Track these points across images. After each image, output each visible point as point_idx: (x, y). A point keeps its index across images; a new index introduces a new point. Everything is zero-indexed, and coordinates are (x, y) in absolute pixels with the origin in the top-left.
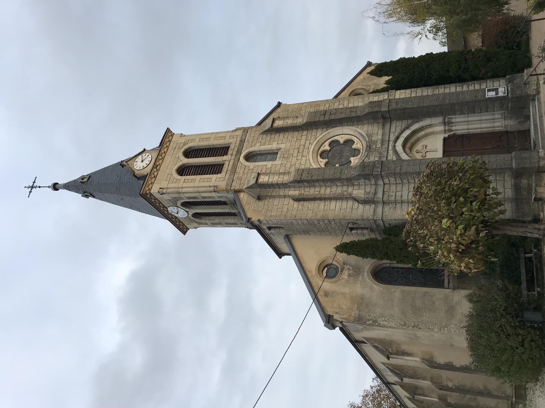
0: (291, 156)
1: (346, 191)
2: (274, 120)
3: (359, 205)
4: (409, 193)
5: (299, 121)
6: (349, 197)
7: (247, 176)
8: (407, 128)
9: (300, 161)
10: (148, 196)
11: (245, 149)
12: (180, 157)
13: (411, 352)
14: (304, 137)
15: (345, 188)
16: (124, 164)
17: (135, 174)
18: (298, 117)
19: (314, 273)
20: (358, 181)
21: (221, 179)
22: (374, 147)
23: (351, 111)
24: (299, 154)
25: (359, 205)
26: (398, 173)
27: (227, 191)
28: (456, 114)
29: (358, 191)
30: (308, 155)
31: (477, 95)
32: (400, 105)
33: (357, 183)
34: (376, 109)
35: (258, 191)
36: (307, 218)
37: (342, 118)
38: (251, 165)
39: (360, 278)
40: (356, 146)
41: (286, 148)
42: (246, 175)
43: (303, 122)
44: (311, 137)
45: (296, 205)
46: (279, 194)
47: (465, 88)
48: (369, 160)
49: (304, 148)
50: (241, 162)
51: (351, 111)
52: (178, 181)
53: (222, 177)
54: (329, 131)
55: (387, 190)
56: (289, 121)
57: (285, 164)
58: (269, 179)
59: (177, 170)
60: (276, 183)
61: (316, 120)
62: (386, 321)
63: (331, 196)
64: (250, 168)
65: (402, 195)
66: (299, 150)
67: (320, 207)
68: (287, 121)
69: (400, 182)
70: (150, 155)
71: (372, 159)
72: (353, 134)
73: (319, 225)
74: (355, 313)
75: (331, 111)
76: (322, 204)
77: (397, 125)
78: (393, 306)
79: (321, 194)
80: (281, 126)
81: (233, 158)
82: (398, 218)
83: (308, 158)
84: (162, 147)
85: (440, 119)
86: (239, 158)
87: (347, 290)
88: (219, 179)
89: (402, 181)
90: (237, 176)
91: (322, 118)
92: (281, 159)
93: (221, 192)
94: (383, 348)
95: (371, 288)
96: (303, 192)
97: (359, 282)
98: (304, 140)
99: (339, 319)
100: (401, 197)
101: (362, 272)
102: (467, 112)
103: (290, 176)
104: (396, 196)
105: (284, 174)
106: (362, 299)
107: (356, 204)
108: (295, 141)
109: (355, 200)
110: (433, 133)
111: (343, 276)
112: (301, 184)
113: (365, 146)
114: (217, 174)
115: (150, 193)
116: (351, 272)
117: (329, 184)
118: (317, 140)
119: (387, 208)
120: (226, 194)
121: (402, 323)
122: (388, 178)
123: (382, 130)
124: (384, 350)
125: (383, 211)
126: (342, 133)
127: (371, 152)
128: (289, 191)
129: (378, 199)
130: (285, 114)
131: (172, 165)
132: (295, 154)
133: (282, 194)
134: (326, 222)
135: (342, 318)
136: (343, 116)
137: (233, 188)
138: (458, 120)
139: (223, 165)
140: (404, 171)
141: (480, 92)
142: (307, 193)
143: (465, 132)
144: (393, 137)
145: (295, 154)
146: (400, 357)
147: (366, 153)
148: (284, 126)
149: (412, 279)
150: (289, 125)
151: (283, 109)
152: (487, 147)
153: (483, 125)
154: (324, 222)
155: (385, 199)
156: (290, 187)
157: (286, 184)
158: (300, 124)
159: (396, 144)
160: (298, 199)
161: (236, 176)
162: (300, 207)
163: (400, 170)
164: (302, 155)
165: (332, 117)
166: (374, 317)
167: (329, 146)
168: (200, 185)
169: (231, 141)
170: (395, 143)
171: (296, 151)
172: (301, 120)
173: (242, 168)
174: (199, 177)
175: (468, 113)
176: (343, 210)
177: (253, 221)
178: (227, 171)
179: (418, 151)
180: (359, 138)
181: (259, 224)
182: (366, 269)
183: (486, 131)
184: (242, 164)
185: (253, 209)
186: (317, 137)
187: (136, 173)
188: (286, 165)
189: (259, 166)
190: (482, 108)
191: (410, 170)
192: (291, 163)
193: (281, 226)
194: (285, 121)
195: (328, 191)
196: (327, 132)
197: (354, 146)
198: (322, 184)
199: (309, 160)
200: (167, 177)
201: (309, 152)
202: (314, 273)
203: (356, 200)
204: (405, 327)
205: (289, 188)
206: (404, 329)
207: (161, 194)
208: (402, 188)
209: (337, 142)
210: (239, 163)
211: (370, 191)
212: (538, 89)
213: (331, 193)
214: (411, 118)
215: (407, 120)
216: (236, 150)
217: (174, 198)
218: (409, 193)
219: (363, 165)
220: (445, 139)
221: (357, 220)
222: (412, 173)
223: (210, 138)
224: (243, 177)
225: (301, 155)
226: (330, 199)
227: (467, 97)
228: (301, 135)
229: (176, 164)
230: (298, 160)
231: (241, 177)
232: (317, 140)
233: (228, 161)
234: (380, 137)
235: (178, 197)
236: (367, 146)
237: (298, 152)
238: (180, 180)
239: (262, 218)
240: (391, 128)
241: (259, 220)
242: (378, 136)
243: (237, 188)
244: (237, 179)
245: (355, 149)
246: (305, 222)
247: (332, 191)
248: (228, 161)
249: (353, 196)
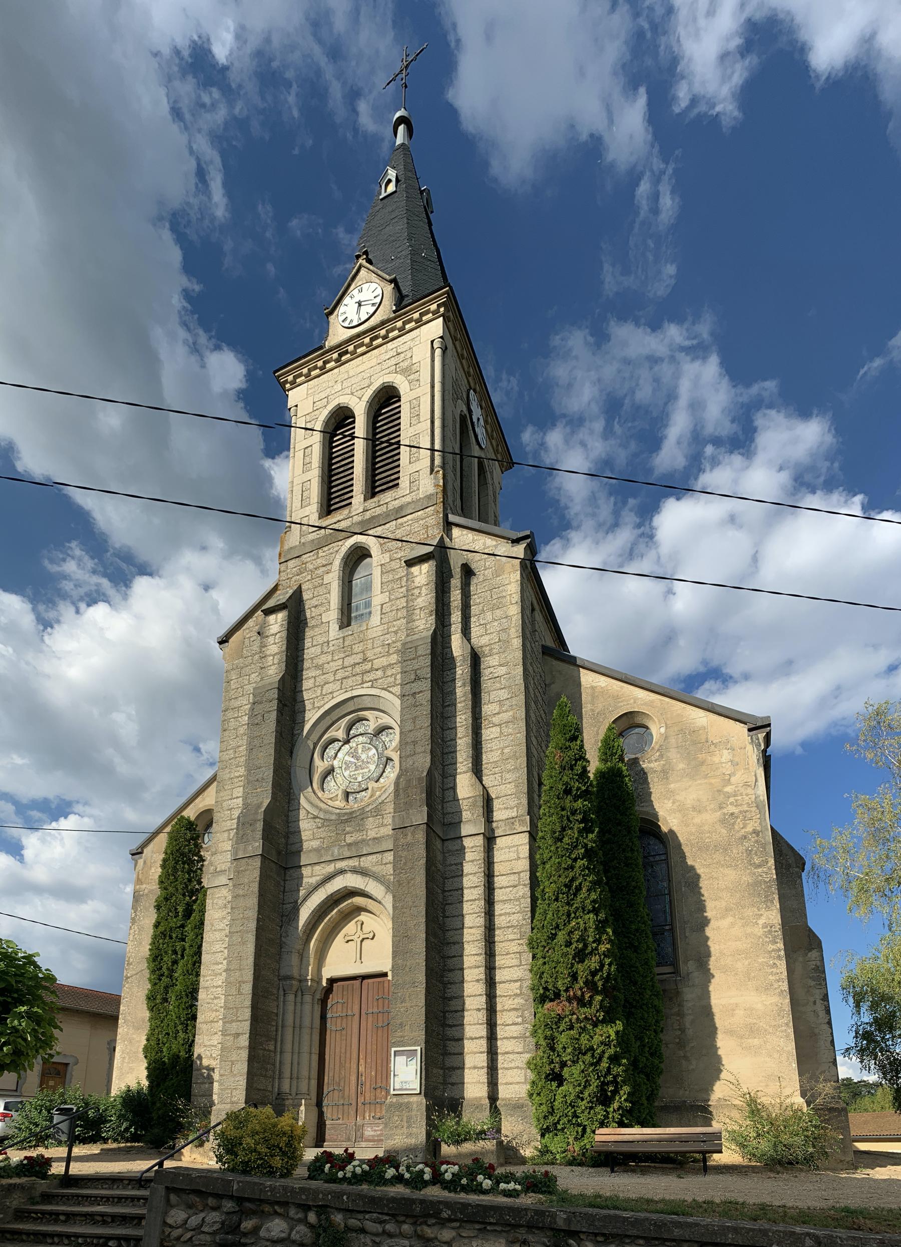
24: (351, 668)
66: (358, 664)
171: (358, 658)
184: (337, 551)
199: (333, 698)
201: (352, 690)
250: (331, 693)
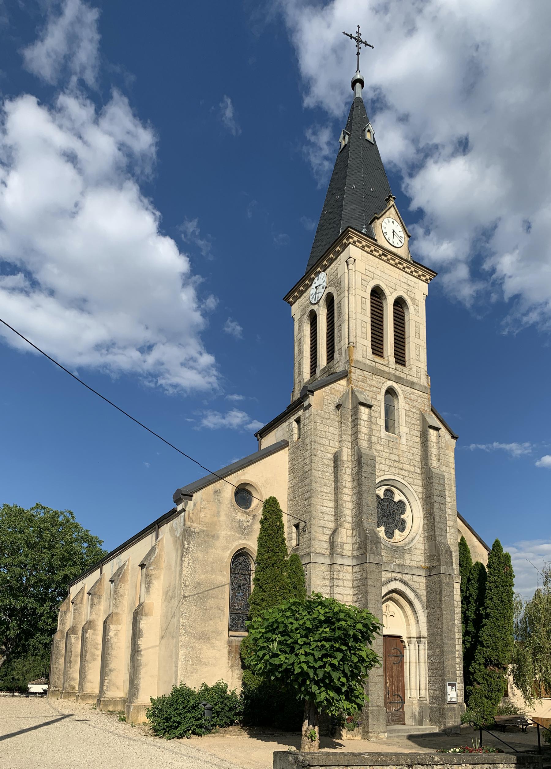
0: (391, 451)
1: (345, 521)
2: (437, 429)
3: (328, 536)
4: (342, 594)
5: (434, 463)
6: (337, 523)
7: (368, 390)
8: (417, 595)
9: (384, 462)
10: (345, 241)
11: (402, 389)
12: (396, 291)
13: (151, 591)
14: (412, 468)
15: (349, 519)
16: (391, 202)
17: (376, 221)
18: (439, 461)
19: (242, 478)
20: (357, 534)
21: (364, 353)
22: (396, 556)
23: (442, 529)
24: (393, 462)
25: (328, 536)
26: (367, 582)
27: (349, 361)
28: (429, 650)
29: (345, 535)
30: (390, 473)
32: (446, 587)
33: (354, 534)
34: (443, 560)
35: (349, 405)
36: (313, 471)
37: (434, 518)
38: (381, 397)
39: (237, 535)
40: (398, 535)
41: (401, 445)
42: (368, 388)
43: (433, 468)
44: (412, 478)
45: (329, 456)
46: (344, 434)
47: (458, 660)
49: (400, 469)
50: (385, 382)
51: (442, 529)
52: (364, 287)
53: (368, 355)
54: (418, 501)
55: (345, 569)
56: (435, 450)
57: (381, 443)
58: (364, 420)
59: (379, 287)
60: (358, 430)
61: (434, 484)
62: (188, 564)
63: (340, 502)
64: (377, 395)
65: (339, 586)
66: (397, 461)
67: (326, 487)
68: (435, 447)
69: (355, 585)
70: (402, 244)
71: (383, 553)
72: (413, 531)
73: (303, 485)
74: (196, 527)
75: (443, 504)
76: (331, 490)
77: (420, 584)
78: (207, 572)
79: (342, 489)
80: (429, 439)
81: (392, 371)
82: (312, 581)
83: (386, 473)
84: (412, 264)
85: (424, 632)
86: (390, 380)
87: (223, 518)
88: (365, 350)
89: (356, 587)
90: (368, 377)
91: (435, 492)
92: (387, 438)
93: (347, 353)
94: (153, 559)
95: (225, 548)
96: (345, 466)
97: (233, 533)
98: (409, 469)
99: (187, 507)
100: (337, 586)
101: (245, 538)
102: (430, 661)
103: (367, 449)
104: (338, 579)
105: (370, 441)
106: (213, 536)
107: (329, 532)
108: (409, 457)
109: (335, 532)
110: (408, 624)
111: (239, 514)
112: (355, 463)
113: (398, 545)
114: (372, 348)
115: (349, 244)
116: (245, 524)
117: (355, 499)
118: (409, 486)
119: (324, 568)
120: (343, 360)
121: (187, 583)
122: (360, 571)
124: (151, 561)
126: (414, 517)
128: (347, 448)
129: (335, 558)
130: (443, 445)
131: (386, 280)
132: (392, 457)
133: (343, 438)
134: (307, 495)
135: (189, 512)
136: (437, 519)
137: (353, 369)
138: (422, 652)
139: (382, 357)
140: (369, 590)
142: (344, 471)
143: (406, 659)
144: (406, 578)
145: (392, 457)
146: (144, 579)
147: (389, 546)
148: (429, 442)
149: (237, 596)
150: (430, 449)
151: (449, 442)
153: (413, 679)
154: (308, 492)
155: (335, 566)
156: (353, 448)
157: (357, 444)
158: (430, 464)
159: (398, 582)
160: (337, 459)
161: (368, 375)
162: (326, 462)
163: (371, 586)
164: (390, 466)
165: (436, 506)
166: (193, 550)
167: (399, 501)
168: (359, 322)
169: (414, 370)
171: (396, 458)
172: (435, 465)
173: (378, 383)
174: (369, 320)
175: (429, 663)
176: (322, 516)
177: (309, 397)
178: (375, 362)
179: (388, 606)
180: (407, 538)
181: (305, 406)
182: (247, 542)
183: (407, 681)
184: (383, 383)
185: (325, 397)
186: (412, 486)
187: (378, 222)
188: (380, 444)
189: (380, 407)
190: (434, 678)
191: (370, 597)
192: (381, 451)
193: (301, 436)
194: (435, 444)
195: (347, 498)
196: (417, 498)
197: (397, 532)
198: (355, 490)
199: (385, 475)
200: (369, 271)
202: (241, 478)
203: (333, 532)
204: (183, 586)
205: (350, 447)
206: (181, 585)
207: (346, 261)
208: (347, 587)
209: (404, 511)
210: (385, 380)
211: (345, 550)
213: (343, 502)
214: (428, 601)
215: (427, 595)
216: (401, 376)
217: (341, 282)
218: (342, 594)
219: (377, 541)
221: (310, 532)
222: (366, 599)
223: (419, 339)
224: (366, 385)
225: (391, 464)
226: (336, 501)
228: (415, 464)
229: (387, 286)
230: (385, 461)
231: (366, 381)
232: (409, 486)
233: (388, 364)
234: (407, 563)
235: (341, 288)
236: (398, 547)
237: (395, 461)
238: (366, 292)
239: (312, 409)
240: (417, 576)
241: (310, 405)
243: (353, 376)
244: (364, 377)
245: (393, 533)
246: (308, 468)
247: (345, 502)
248: (388, 364)
249: (340, 529)
250: (384, 471)
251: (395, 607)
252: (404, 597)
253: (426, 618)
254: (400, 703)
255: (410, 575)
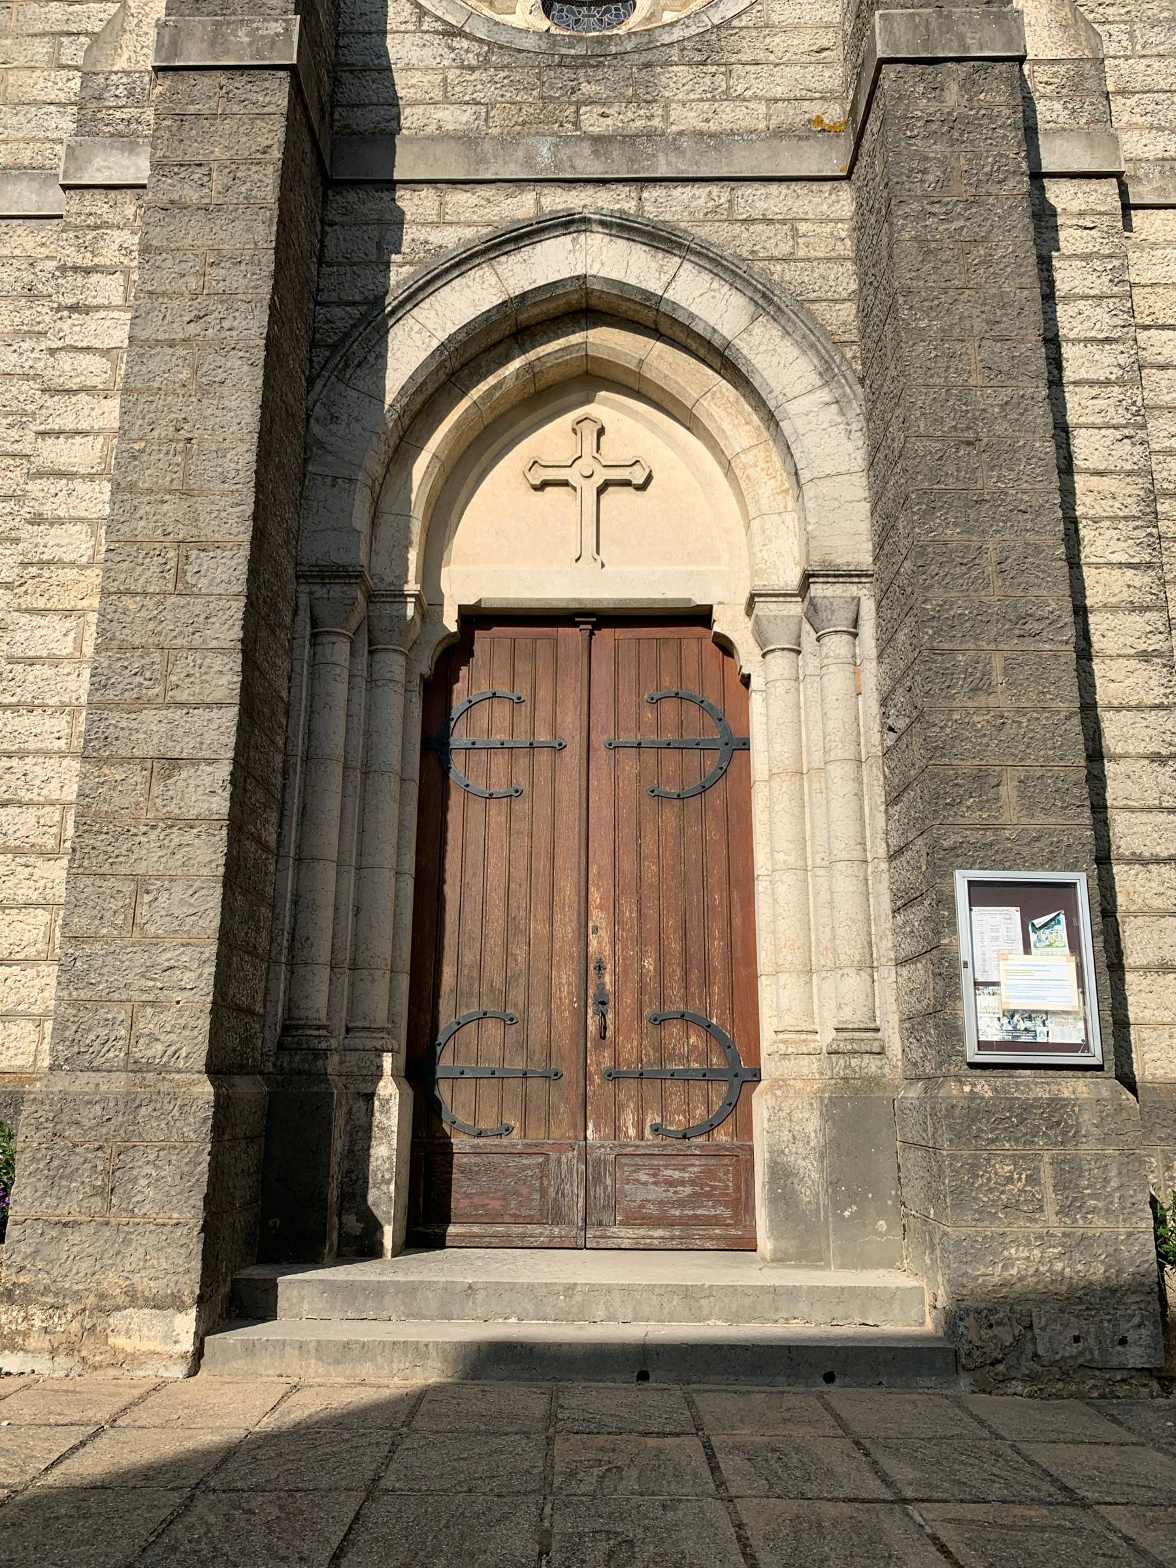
31: (1008, 791)
48: (463, 67)
77: (803, 227)
123: (762, 126)
125: (15, 222)
127: (539, 76)
141: (1041, 818)
152: (598, 917)
170: (603, 223)
212: (1031, 1378)
220: (701, 616)
227: (981, 700)
240: (774, 188)
242: (706, 106)
251: (654, 427)
252: (682, 337)
253: (859, 440)
254: (708, 1076)
255: (715, 189)
